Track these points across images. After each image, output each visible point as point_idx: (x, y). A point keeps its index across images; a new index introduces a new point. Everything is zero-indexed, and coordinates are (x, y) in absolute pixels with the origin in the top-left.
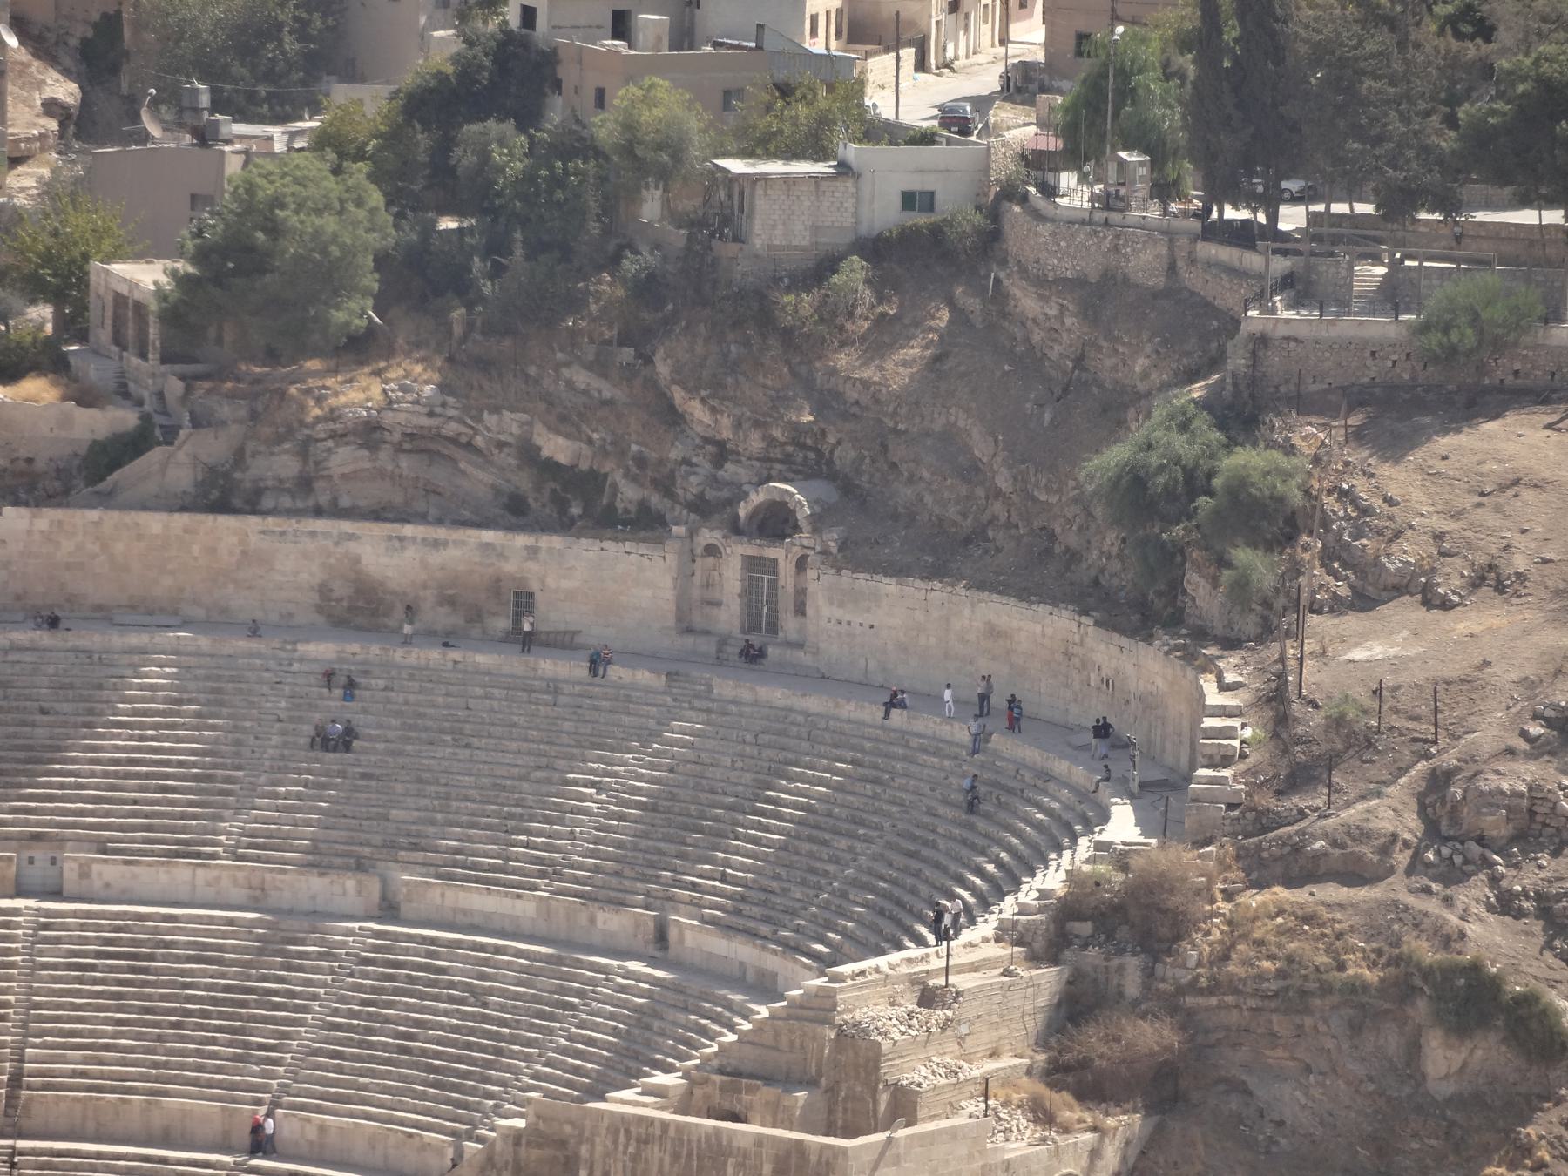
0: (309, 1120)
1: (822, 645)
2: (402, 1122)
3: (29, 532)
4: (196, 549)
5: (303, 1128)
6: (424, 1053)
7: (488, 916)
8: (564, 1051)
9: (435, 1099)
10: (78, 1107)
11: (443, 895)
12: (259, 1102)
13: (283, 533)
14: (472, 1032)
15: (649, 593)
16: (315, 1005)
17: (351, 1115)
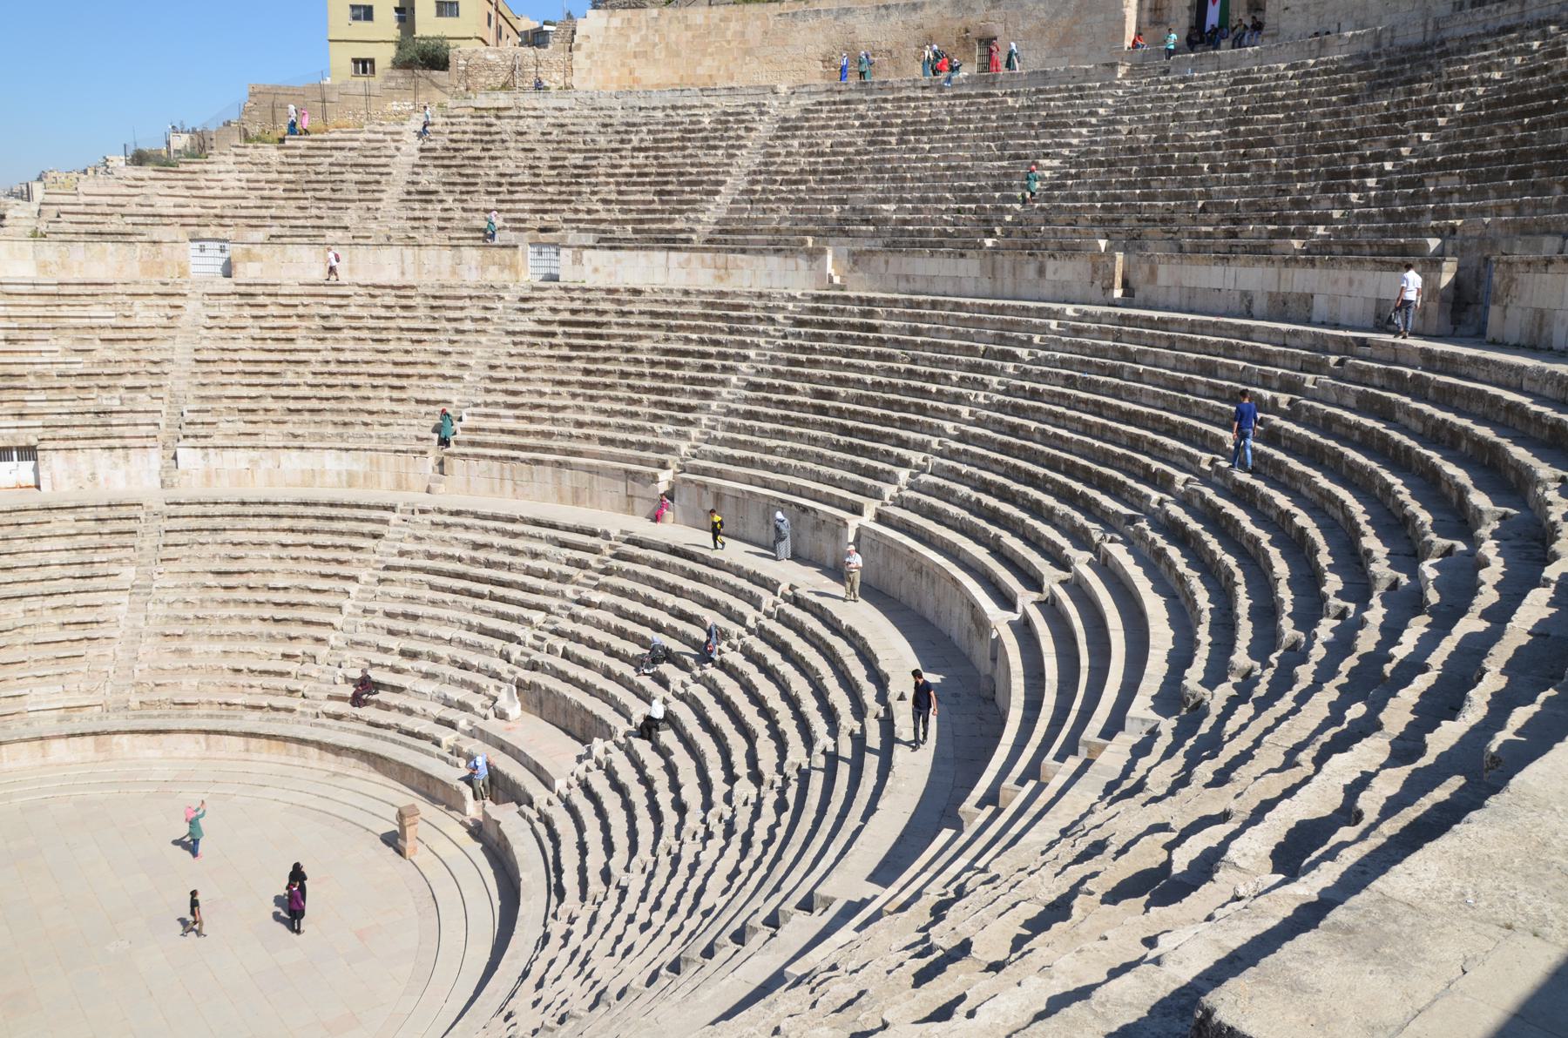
0: (705, 486)
1: (1283, 25)
2: (800, 492)
3: (607, 28)
4: (729, 34)
5: (700, 496)
6: (840, 413)
7: (930, 279)
8: (1000, 407)
9: (842, 465)
10: (496, 464)
11: (887, 262)
12: (663, 465)
13: (794, 14)
14: (893, 388)
15: (1100, 17)
16: (743, 366)
17: (750, 481)
